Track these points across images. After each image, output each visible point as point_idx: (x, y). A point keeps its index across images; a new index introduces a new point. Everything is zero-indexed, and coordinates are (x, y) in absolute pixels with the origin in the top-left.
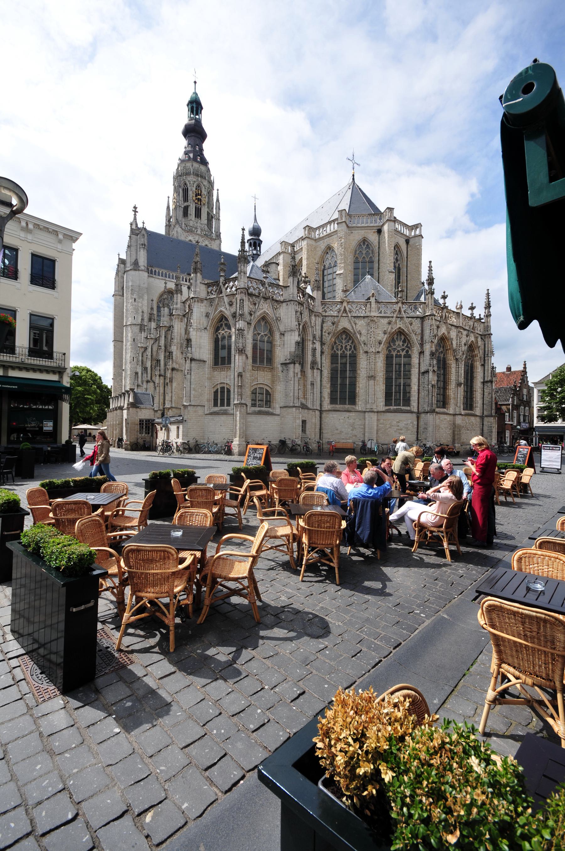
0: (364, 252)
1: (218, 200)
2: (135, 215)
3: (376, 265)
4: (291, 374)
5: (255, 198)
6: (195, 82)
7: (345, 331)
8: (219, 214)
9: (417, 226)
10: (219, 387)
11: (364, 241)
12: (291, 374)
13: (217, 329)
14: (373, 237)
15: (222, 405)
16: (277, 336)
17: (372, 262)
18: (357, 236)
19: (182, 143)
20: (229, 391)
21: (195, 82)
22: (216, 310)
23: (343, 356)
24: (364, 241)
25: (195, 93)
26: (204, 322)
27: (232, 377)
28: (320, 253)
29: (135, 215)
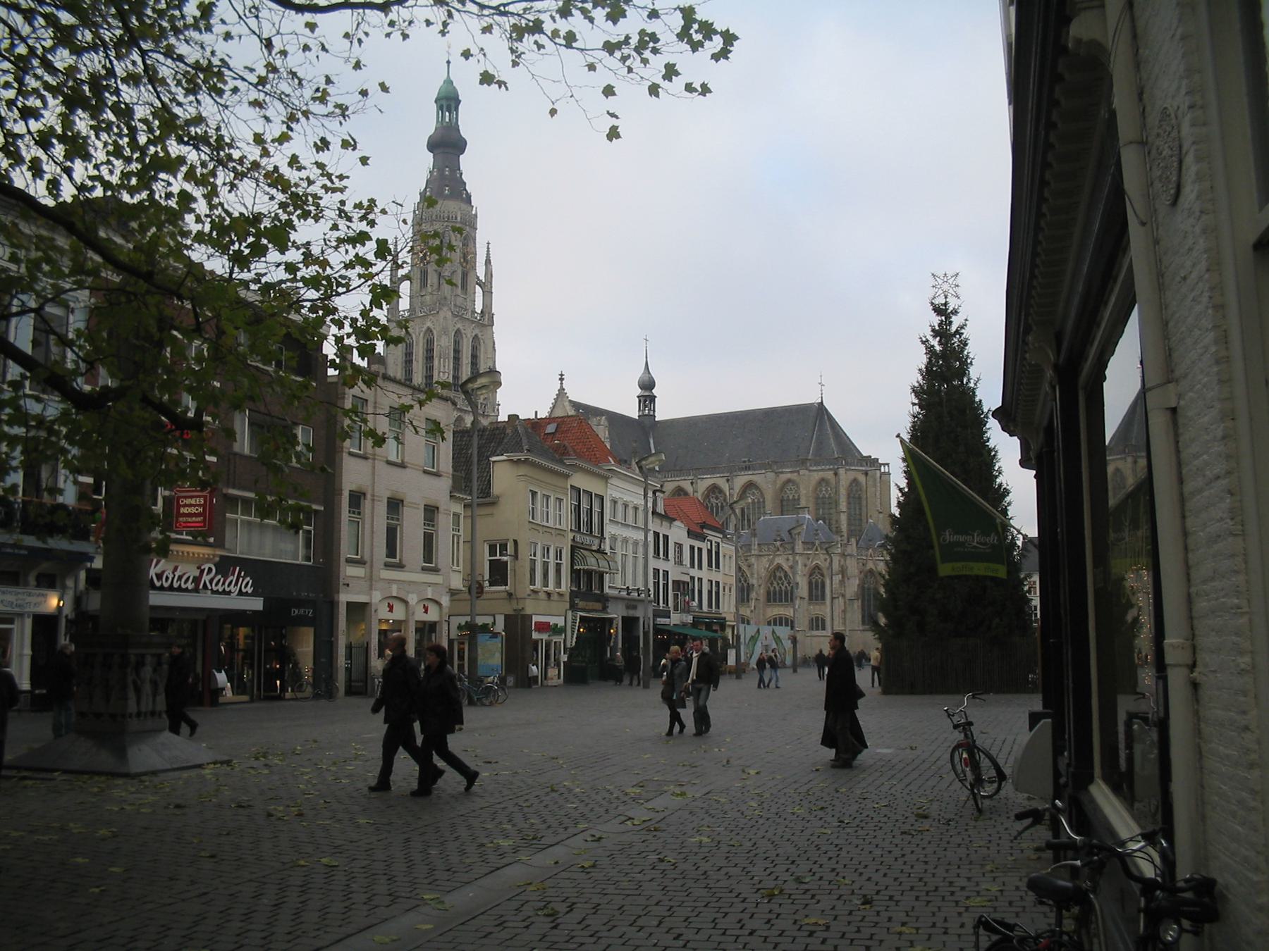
0: (854, 489)
1: (488, 262)
2: (562, 384)
3: (864, 503)
4: (856, 606)
5: (646, 340)
6: (448, 62)
7: (871, 571)
8: (491, 284)
9: (888, 464)
10: (814, 617)
11: (855, 480)
12: (856, 606)
13: (811, 575)
14: (862, 478)
15: (817, 629)
16: (846, 579)
17: (860, 498)
18: (851, 475)
19: (427, 160)
20: (823, 621)
21: (448, 62)
22: (812, 562)
23: (869, 589)
24: (855, 480)
25: (449, 82)
26: (806, 570)
27: (828, 610)
28: (813, 483)
29: (562, 384)
